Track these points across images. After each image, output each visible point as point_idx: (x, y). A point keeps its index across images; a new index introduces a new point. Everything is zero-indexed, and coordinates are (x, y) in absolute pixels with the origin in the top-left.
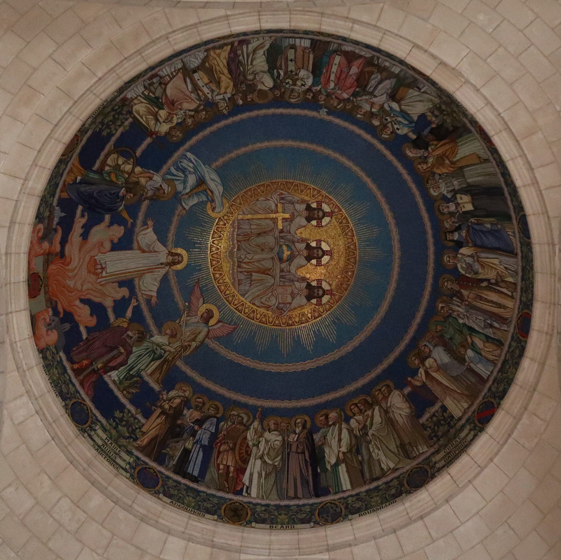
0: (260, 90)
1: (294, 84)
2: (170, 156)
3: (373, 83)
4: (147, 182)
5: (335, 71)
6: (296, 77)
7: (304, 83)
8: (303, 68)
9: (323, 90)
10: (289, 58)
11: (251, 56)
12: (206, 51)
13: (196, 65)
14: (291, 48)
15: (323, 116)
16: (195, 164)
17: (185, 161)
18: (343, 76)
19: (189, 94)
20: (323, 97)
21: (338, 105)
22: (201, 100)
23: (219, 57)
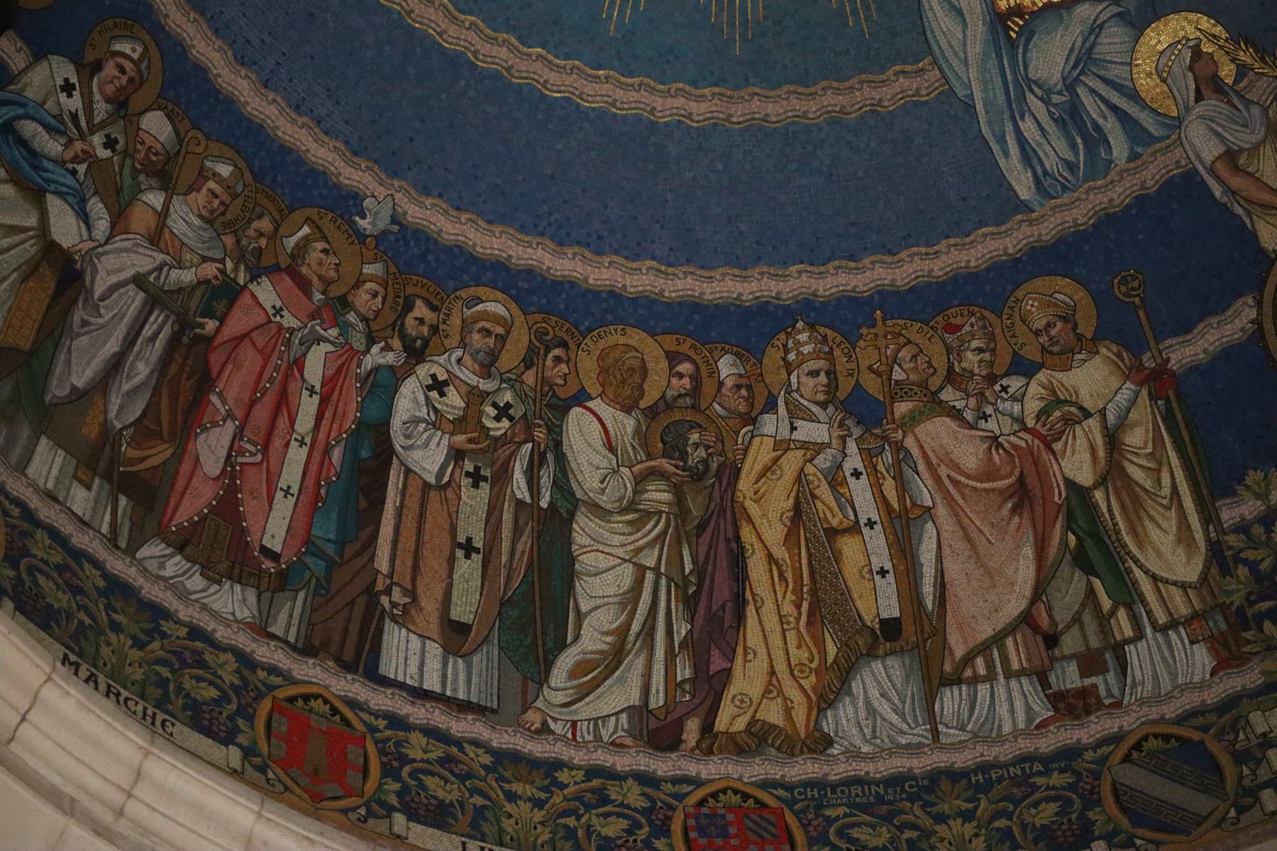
0: (627, 410)
1: (475, 397)
2: (1108, 222)
3: (142, 368)
4: (1256, 147)
5: (294, 444)
6: (460, 439)
7: (434, 394)
8: (426, 485)
9: (358, 342)
10: (477, 558)
11: (635, 627)
12: (820, 743)
13: (877, 666)
14: (462, 629)
15: (381, 192)
16: (1009, 128)
17: (1051, 163)
18: (261, 414)
19: (942, 512)
20: (363, 299)
21: (303, 247)
22: (899, 447)
23: (772, 672)
